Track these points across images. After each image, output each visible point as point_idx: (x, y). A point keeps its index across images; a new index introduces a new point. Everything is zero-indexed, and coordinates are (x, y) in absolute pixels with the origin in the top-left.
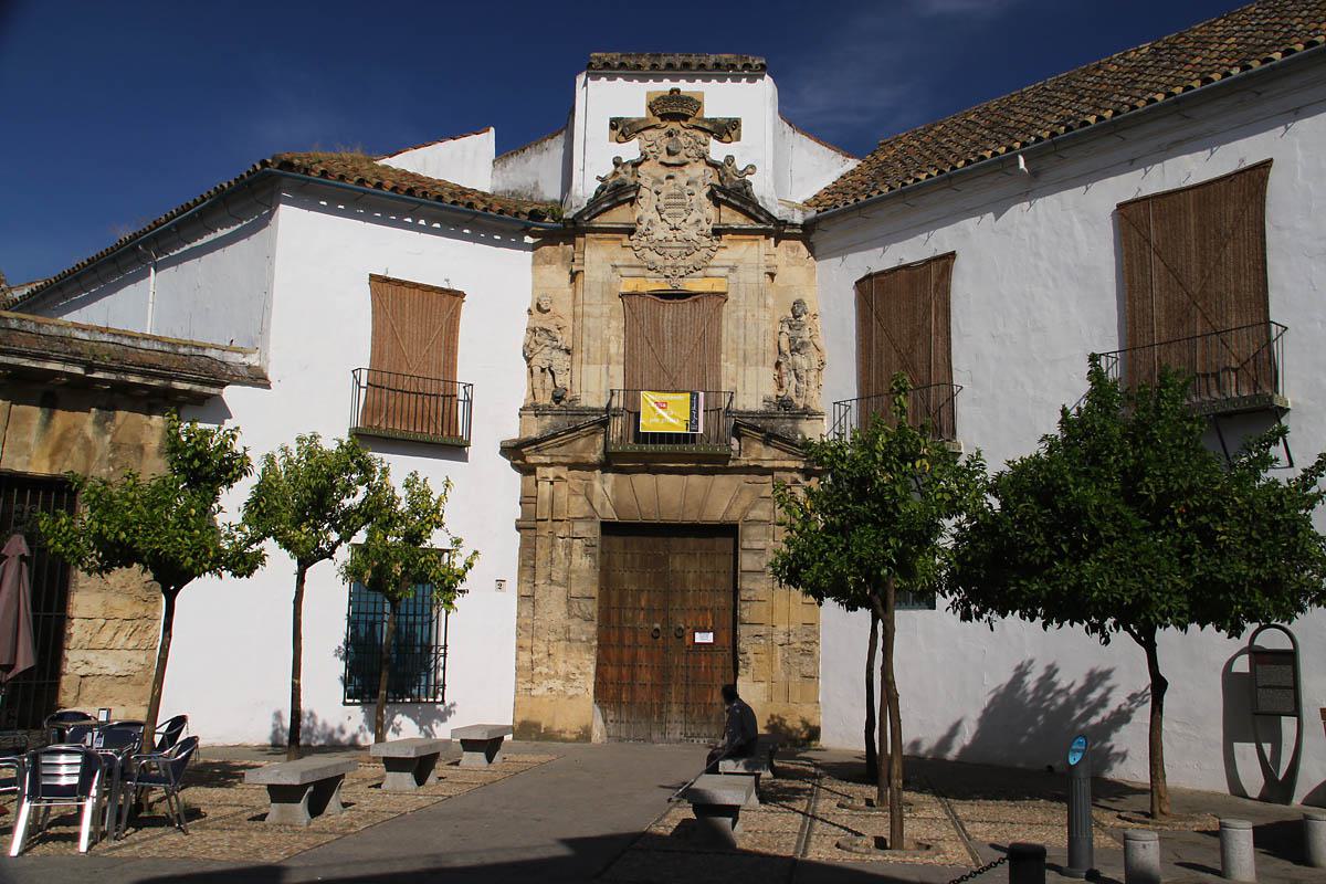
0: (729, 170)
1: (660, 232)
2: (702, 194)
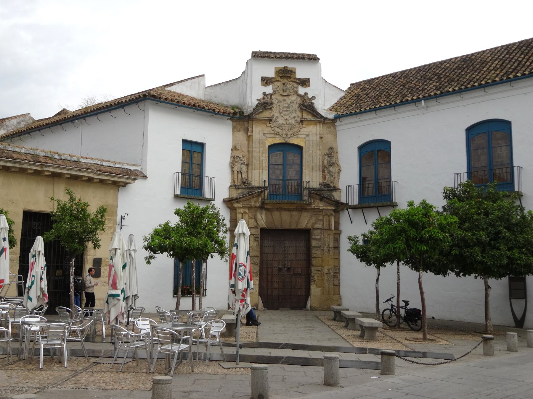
0: (306, 98)
1: (281, 121)
2: (296, 106)
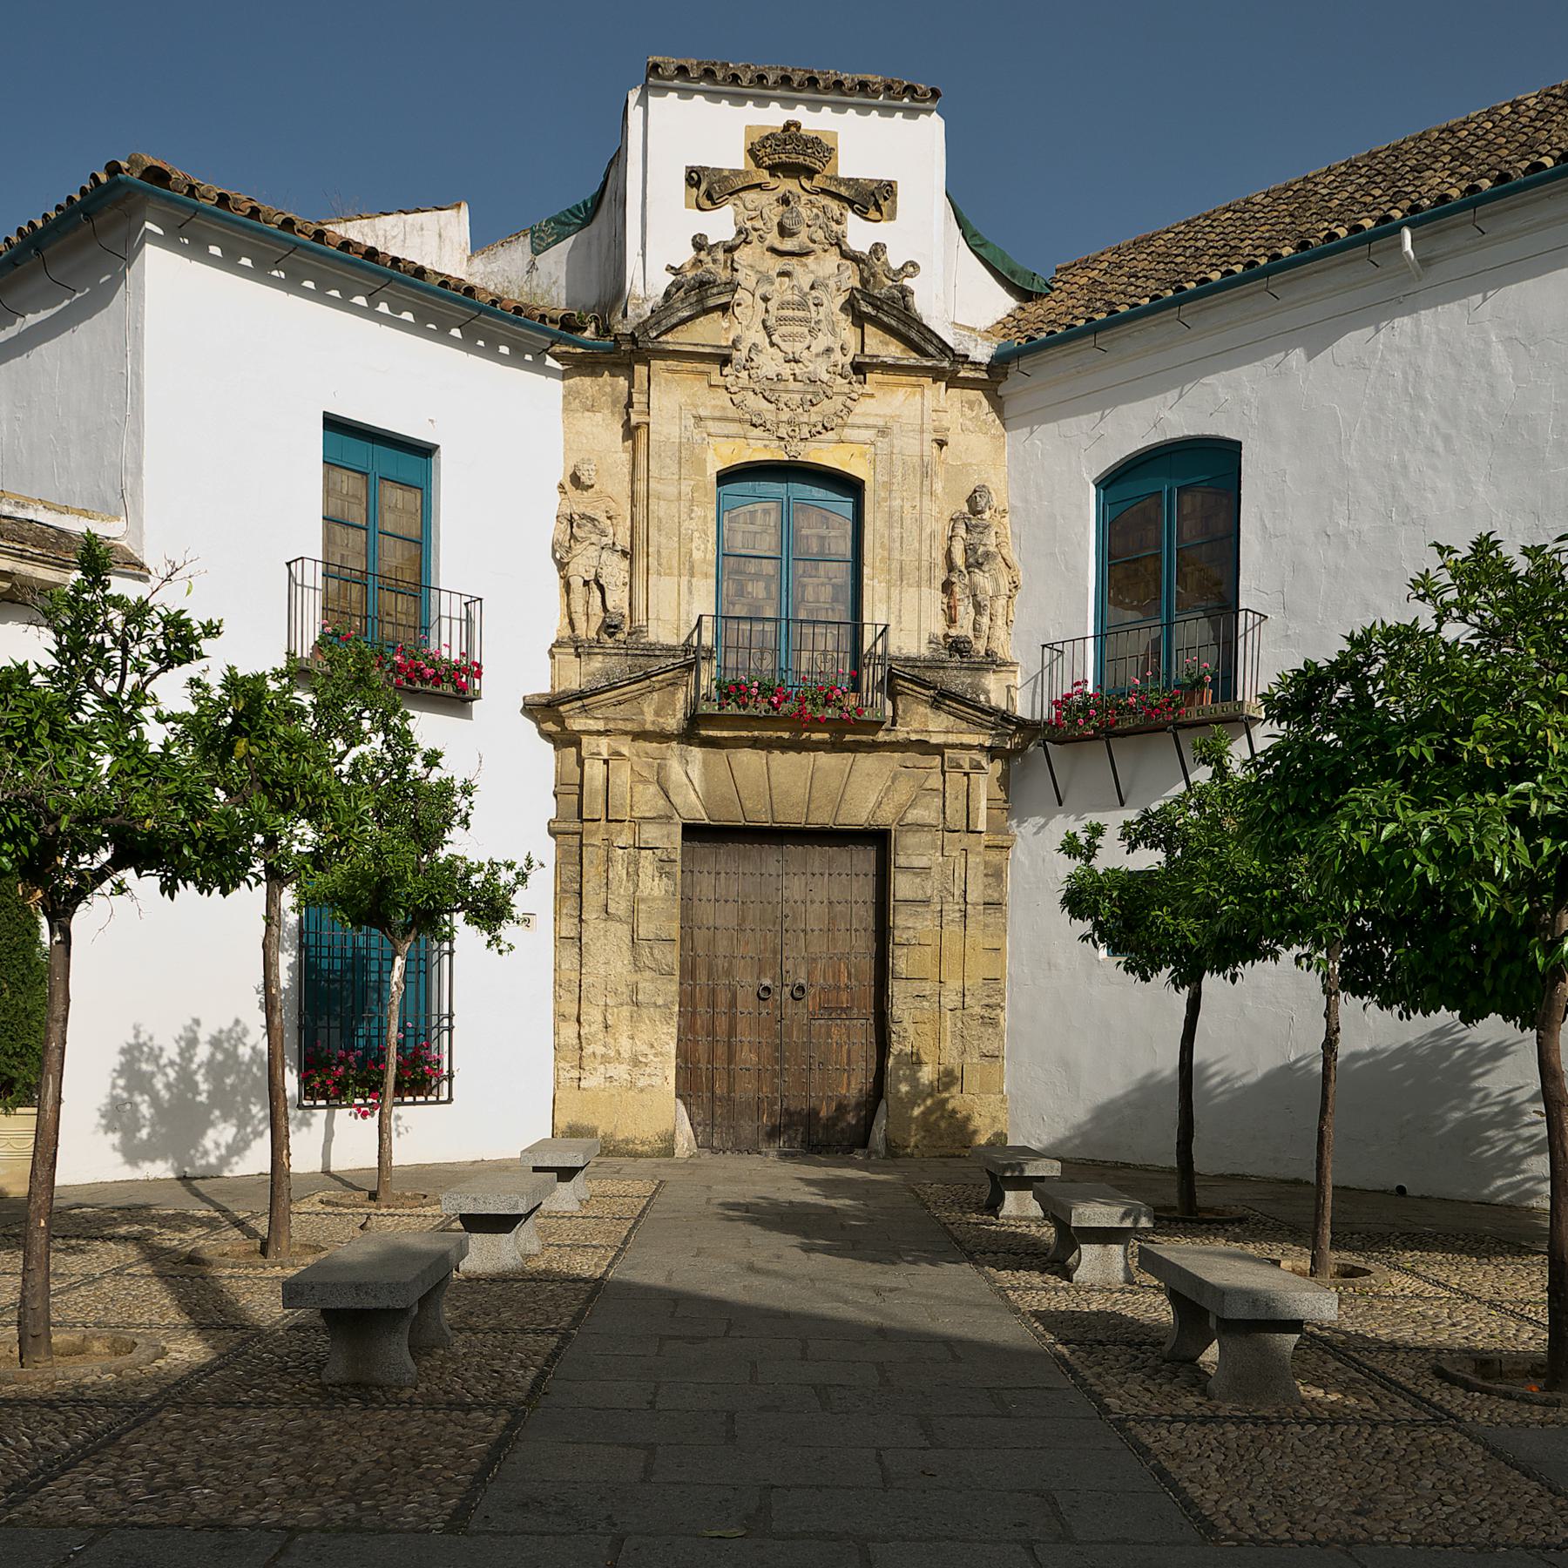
1: (770, 363)
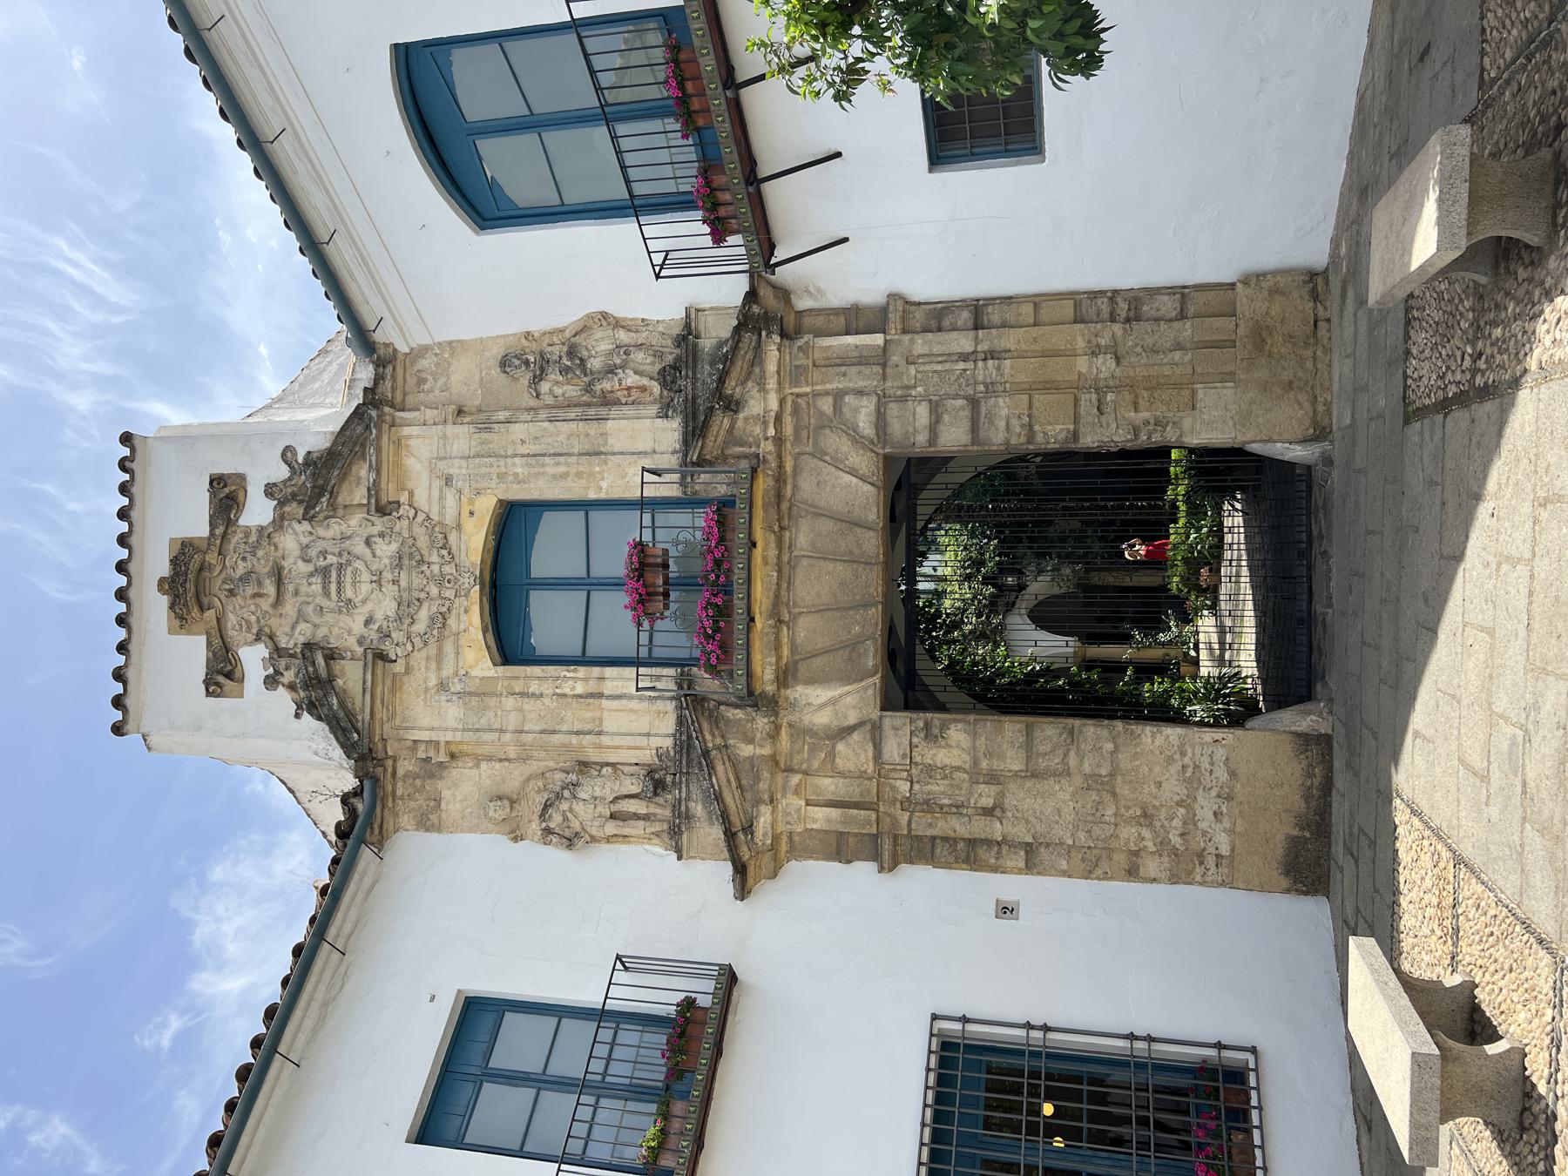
1: (386, 606)
